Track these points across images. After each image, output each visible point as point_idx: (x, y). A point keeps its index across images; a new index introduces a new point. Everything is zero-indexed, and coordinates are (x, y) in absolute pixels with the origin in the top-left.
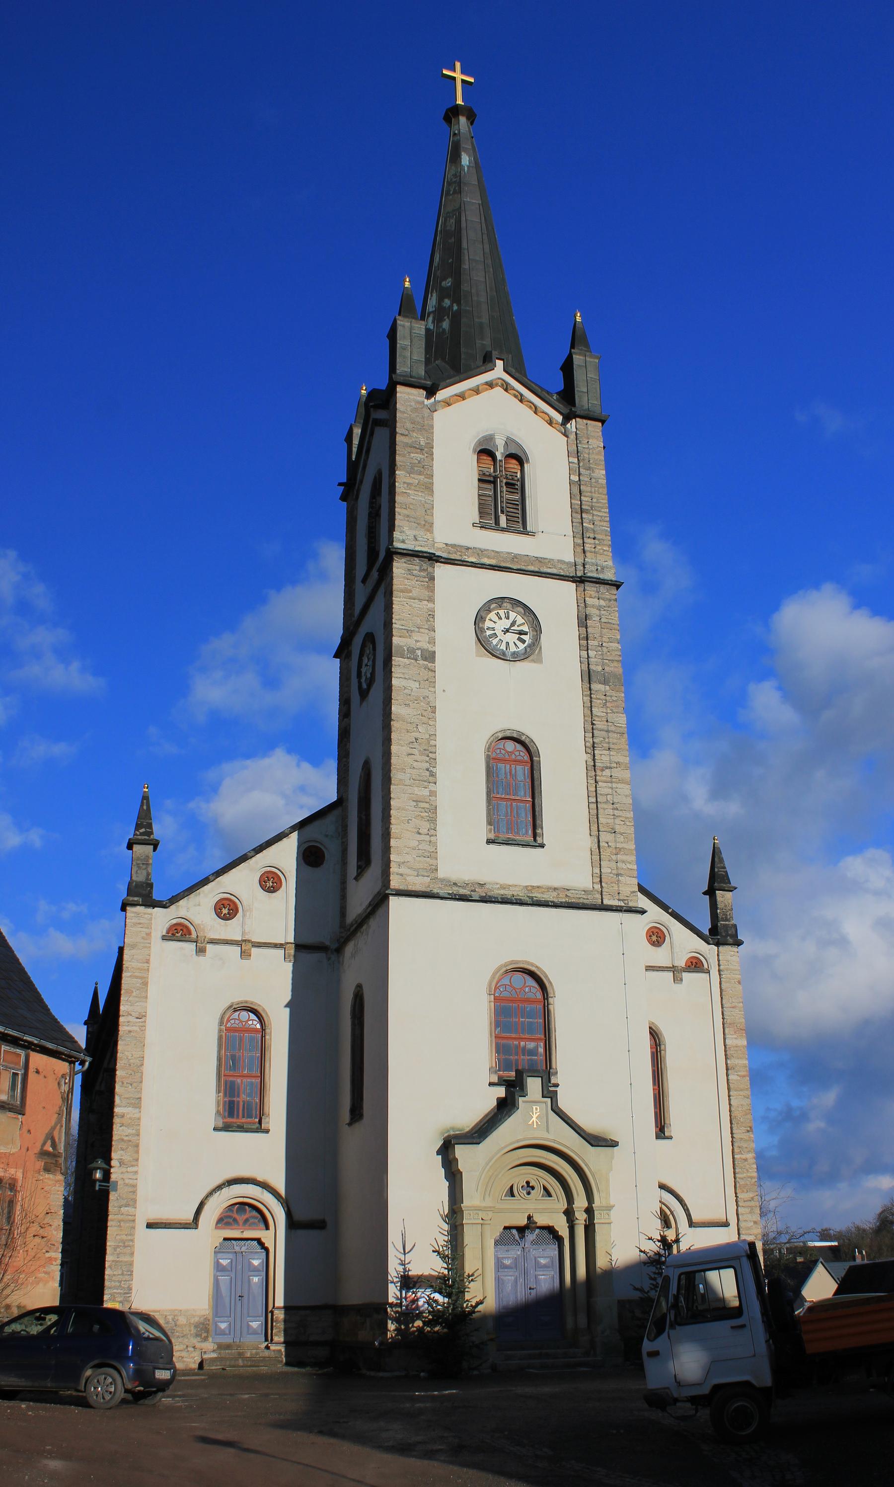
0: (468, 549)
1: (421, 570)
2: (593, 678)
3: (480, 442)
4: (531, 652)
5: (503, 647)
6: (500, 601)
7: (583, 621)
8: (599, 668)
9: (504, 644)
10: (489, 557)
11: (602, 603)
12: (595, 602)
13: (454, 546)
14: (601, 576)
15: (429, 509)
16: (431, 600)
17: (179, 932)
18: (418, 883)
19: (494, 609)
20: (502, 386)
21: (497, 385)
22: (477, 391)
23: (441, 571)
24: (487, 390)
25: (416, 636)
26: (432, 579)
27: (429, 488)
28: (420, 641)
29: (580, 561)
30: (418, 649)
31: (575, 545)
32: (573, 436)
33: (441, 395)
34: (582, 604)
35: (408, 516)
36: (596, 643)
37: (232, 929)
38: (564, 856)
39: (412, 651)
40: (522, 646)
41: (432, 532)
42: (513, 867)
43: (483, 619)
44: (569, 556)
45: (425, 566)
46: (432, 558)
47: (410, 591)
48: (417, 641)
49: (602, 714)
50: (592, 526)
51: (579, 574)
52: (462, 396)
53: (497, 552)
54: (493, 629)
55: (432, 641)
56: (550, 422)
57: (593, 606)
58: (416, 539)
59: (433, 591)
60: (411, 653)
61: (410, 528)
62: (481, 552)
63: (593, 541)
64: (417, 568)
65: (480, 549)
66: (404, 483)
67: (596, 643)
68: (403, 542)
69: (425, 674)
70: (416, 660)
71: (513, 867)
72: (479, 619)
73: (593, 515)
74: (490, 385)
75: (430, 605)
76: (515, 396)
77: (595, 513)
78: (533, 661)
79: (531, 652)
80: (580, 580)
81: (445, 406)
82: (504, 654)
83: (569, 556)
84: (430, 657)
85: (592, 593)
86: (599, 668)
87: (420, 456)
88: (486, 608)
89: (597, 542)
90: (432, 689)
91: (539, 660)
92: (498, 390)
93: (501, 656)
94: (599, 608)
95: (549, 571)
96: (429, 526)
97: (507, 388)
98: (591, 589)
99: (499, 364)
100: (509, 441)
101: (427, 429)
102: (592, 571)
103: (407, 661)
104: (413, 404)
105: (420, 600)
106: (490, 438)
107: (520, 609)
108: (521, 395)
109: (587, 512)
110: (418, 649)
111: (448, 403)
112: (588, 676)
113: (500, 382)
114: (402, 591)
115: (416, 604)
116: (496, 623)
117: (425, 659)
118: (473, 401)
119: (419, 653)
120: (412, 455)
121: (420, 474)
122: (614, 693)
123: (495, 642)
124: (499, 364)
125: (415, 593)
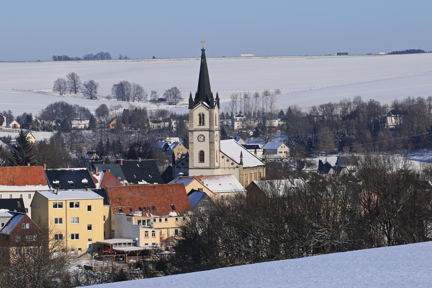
7: (210, 136)
17: (178, 167)
18: (191, 168)
23: (194, 132)
33: (194, 109)
34: (210, 134)
37: (183, 166)
38: (207, 163)
42: (202, 165)
46: (193, 131)
60: (191, 143)
71: (202, 165)
84: (193, 143)
93: (200, 141)
106: (200, 113)
112: (210, 143)
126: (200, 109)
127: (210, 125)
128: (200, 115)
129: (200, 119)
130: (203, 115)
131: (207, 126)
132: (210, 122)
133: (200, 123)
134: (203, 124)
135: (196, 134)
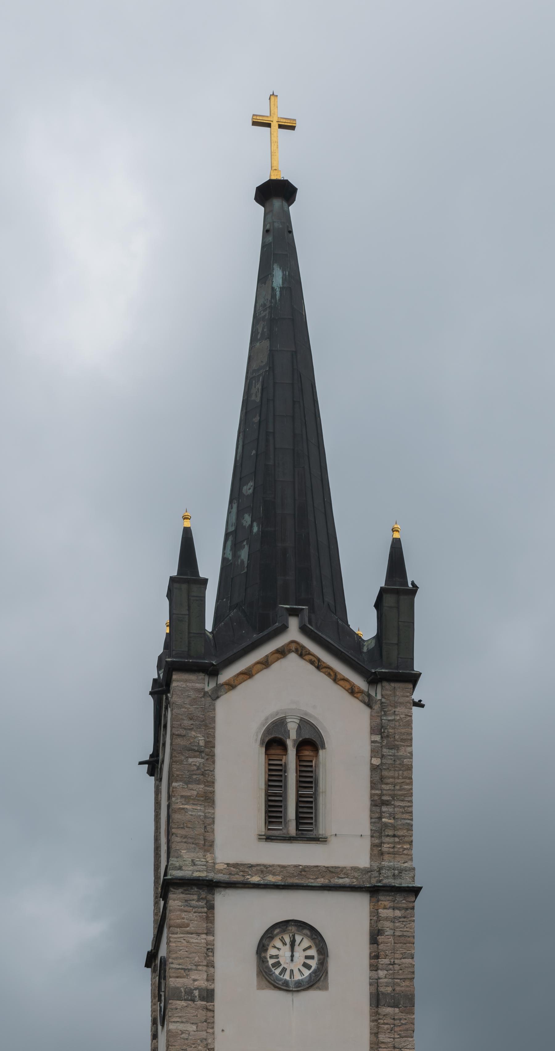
0: (251, 866)
1: (199, 900)
2: (382, 1002)
3: (268, 731)
4: (318, 979)
5: (287, 977)
6: (284, 925)
8: (389, 989)
9: (288, 973)
10: (274, 874)
11: (398, 913)
12: (389, 913)
13: (236, 865)
14: (396, 883)
15: (208, 824)
16: (210, 932)
19: (277, 934)
20: (296, 651)
21: (290, 651)
22: (266, 663)
24: (278, 659)
25: (194, 975)
26: (211, 907)
27: (208, 799)
28: (198, 980)
29: (375, 865)
30: (196, 989)
31: (373, 846)
32: (377, 707)
33: (227, 675)
34: (375, 917)
35: (186, 837)
36: (386, 961)
39: (189, 992)
40: (307, 973)
41: (213, 853)
43: (272, 938)
44: (364, 861)
45: (203, 894)
46: (210, 886)
47: (188, 926)
48: (195, 980)
49: (389, 1040)
50: (392, 821)
51: (374, 882)
52: (248, 674)
53: (284, 867)
54: (277, 957)
55: (211, 978)
56: (353, 691)
57: (387, 919)
58: (193, 863)
59: (212, 922)
60: (189, 995)
61: (188, 849)
62: (264, 869)
63: (392, 840)
64: (195, 897)
65: (265, 866)
66: (182, 797)
67: (386, 961)
68: (180, 868)
69: (202, 1014)
70: (193, 1001)
72: (262, 948)
73: (395, 807)
74: (282, 653)
75: (210, 938)
76: (312, 662)
77: (397, 803)
78: (320, 989)
79: (318, 979)
80: (374, 891)
81: (229, 690)
82: (286, 983)
83: (364, 861)
84: (208, 995)
85: (386, 903)
86: (389, 989)
87: (199, 761)
88: (269, 936)
89: (397, 840)
90: (211, 1031)
91: (326, 988)
92: (293, 657)
93: (284, 987)
94: (393, 920)
95: (341, 881)
96: (208, 845)
97: (302, 653)
98: (385, 900)
99: (294, 623)
100: (304, 723)
101: (207, 724)
102: (387, 877)
103: (183, 1003)
104: (191, 693)
105: (198, 934)
107: (307, 932)
108: (319, 660)
109: (386, 803)
110: (196, 989)
111: (231, 686)
112: (377, 1000)
113: (293, 647)
114: (179, 926)
115: (194, 939)
116: (280, 950)
117: (202, 998)
118: (263, 678)
119: (196, 993)
120: (190, 760)
121: (198, 782)
122: (403, 1016)
123: (277, 972)
124: (294, 623)
125: (191, 928)
126: (286, 685)
127: (379, 831)
128: (273, 743)
129: (275, 777)
130: (311, 743)
131: (346, 839)
132: (378, 803)
133: (273, 811)
134: (307, 828)
135: (240, 918)
